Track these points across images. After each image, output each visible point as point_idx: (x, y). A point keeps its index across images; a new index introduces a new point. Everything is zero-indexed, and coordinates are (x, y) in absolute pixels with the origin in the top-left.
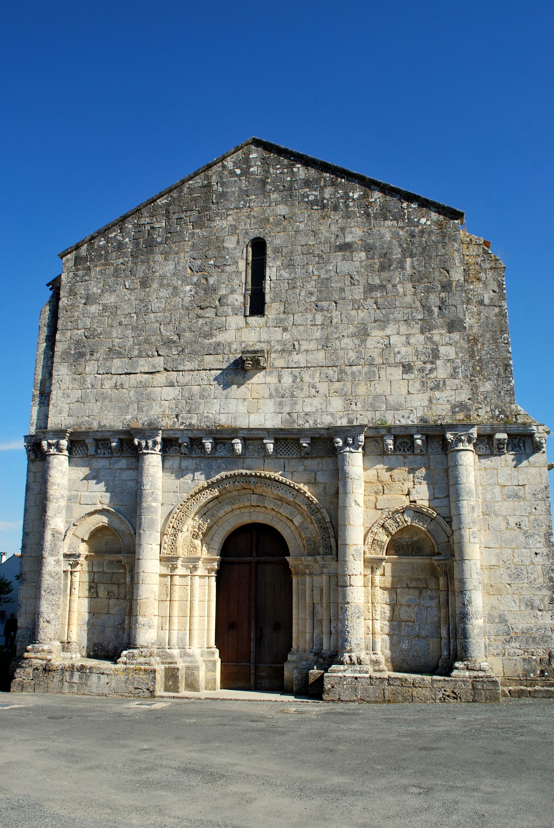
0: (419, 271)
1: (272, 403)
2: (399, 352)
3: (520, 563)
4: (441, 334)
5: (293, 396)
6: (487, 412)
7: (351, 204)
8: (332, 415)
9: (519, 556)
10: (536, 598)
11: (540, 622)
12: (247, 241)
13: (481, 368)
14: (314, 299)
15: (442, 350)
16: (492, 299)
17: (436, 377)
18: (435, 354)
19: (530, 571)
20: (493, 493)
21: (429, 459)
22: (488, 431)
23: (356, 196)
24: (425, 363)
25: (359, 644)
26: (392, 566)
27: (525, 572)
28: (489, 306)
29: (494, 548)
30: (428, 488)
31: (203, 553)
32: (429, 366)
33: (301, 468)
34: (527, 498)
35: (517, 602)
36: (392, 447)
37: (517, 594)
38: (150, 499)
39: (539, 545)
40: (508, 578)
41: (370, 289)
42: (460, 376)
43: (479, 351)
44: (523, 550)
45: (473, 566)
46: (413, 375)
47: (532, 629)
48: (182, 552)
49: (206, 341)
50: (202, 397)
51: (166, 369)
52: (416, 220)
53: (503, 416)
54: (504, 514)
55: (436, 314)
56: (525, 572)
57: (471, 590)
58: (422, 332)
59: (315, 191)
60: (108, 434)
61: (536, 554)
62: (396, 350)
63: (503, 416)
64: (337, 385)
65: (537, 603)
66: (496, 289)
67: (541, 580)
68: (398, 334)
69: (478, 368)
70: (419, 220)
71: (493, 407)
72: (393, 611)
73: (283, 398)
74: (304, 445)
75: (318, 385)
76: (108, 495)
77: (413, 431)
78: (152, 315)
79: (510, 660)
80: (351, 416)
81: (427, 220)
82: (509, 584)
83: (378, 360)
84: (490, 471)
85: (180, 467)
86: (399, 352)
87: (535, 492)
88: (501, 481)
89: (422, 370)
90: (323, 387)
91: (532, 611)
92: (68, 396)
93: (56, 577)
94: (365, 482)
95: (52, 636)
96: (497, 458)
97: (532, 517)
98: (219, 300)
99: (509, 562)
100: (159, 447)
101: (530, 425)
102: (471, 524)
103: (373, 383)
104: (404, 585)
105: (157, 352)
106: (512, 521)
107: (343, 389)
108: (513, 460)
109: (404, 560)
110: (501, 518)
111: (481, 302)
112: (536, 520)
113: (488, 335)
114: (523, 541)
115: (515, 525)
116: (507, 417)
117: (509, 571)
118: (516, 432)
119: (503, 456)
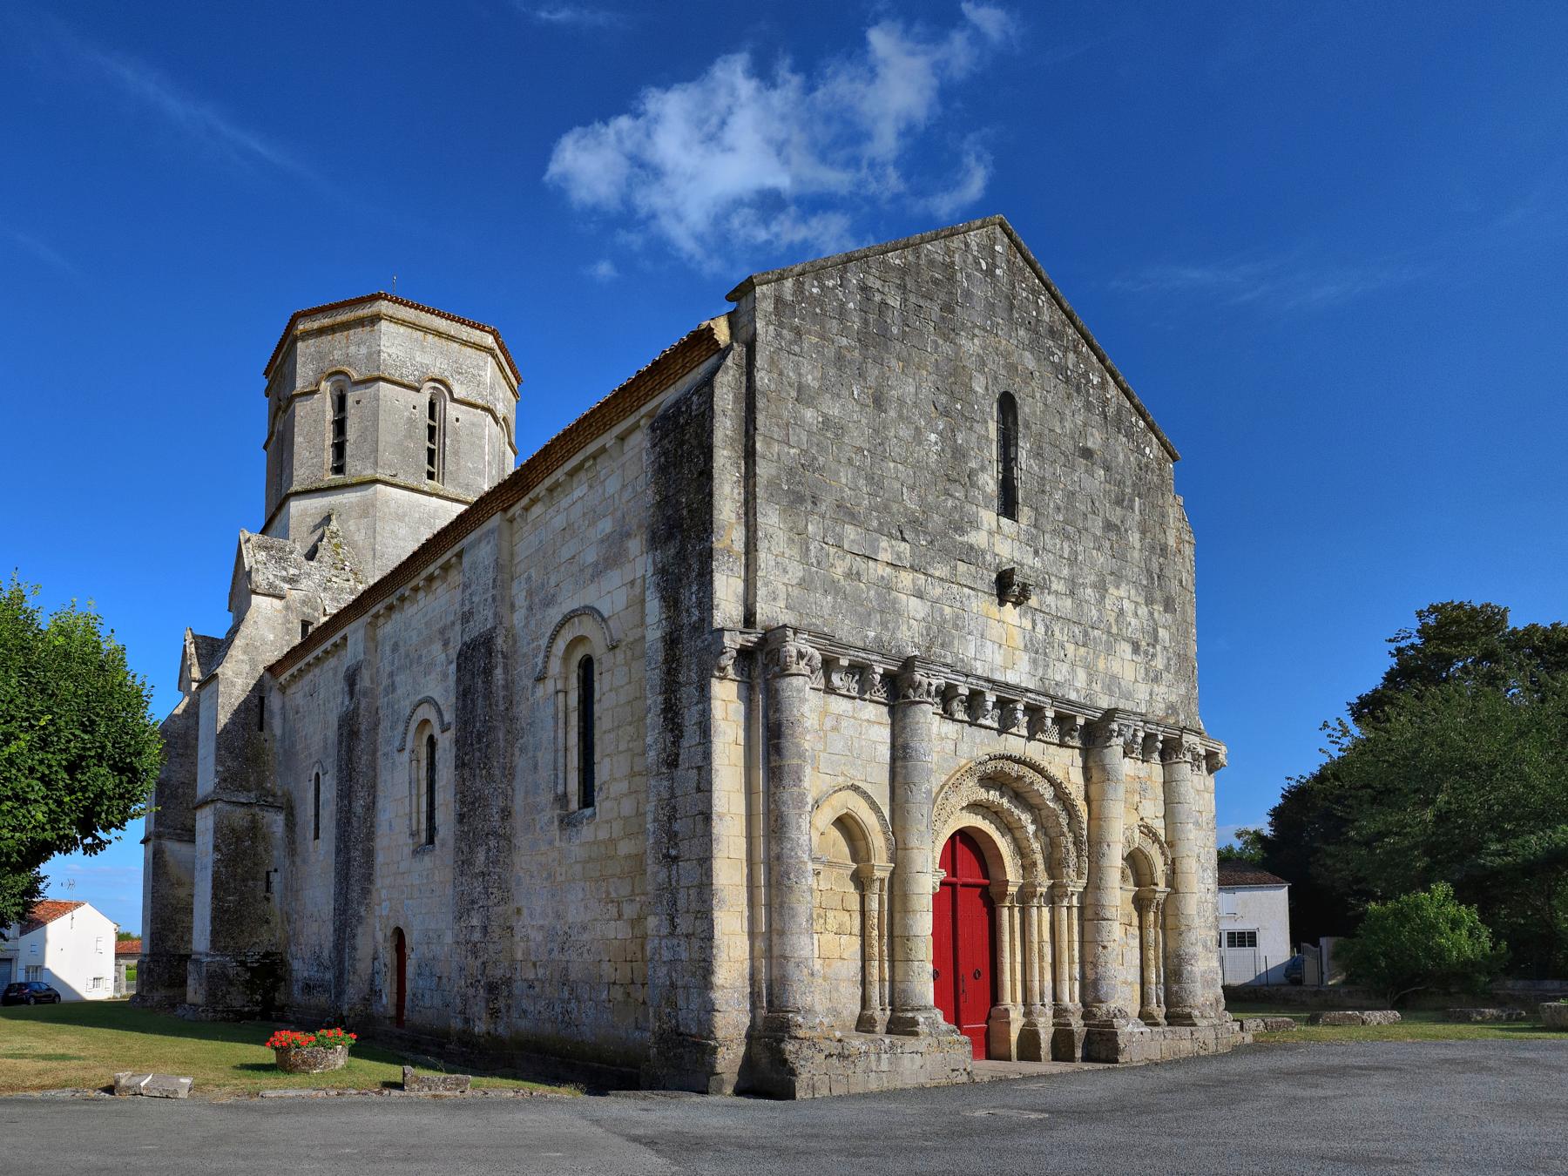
1: (1027, 658)
49: (957, 536)
50: (956, 626)
51: (912, 567)
64: (1082, 650)
78: (892, 465)
92: (785, 571)
98: (969, 477)
105: (901, 532)
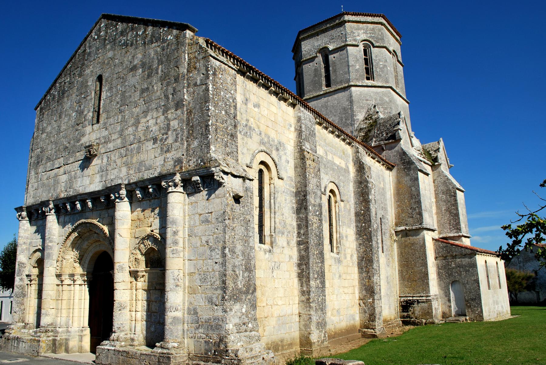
0: (165, 73)
2: (152, 131)
3: (206, 271)
4: (172, 113)
5: (107, 170)
6: (194, 162)
7: (138, 39)
8: (122, 178)
9: (206, 265)
10: (214, 296)
11: (216, 314)
12: (96, 78)
13: (193, 131)
14: (119, 106)
15: (172, 123)
16: (202, 80)
17: (168, 143)
18: (168, 127)
19: (211, 276)
20: (195, 220)
21: (161, 200)
22: (188, 177)
23: (141, 33)
24: (163, 135)
25: (120, 327)
26: (149, 275)
27: (209, 277)
28: (200, 85)
29: (193, 260)
30: (160, 220)
31: (79, 270)
32: (165, 136)
33: (107, 215)
34: (213, 222)
35: (204, 299)
36: (140, 195)
37: (204, 293)
38: (48, 241)
39: (218, 256)
40: (199, 281)
41: (143, 91)
42: (179, 140)
43: (192, 120)
44: (209, 261)
45: (171, 274)
46: (157, 145)
47: (211, 320)
48: (67, 271)
52: (166, 38)
53: (202, 163)
54: (200, 234)
55: (171, 99)
56: (209, 277)
57: (168, 291)
58: (163, 114)
59: (124, 37)
60: (37, 206)
61: (216, 263)
62: (151, 129)
63: (202, 163)
65: (215, 300)
66: (205, 72)
67: (218, 283)
68: (152, 118)
69: (191, 132)
70: (167, 38)
71: (197, 158)
72: (148, 305)
73: (103, 172)
74: (102, 200)
75: (117, 161)
76: (41, 240)
77: (147, 183)
79: (198, 341)
80: (129, 178)
81: (171, 36)
82: (200, 286)
83: (143, 138)
84: (194, 204)
85: (64, 221)
86: (152, 131)
87: (217, 217)
88: (200, 211)
89: (161, 140)
90: (119, 162)
91: (211, 306)
93: (20, 288)
94: (132, 220)
95: (17, 320)
96: (198, 194)
97: (215, 236)
99: (201, 270)
100: (53, 211)
101: (210, 167)
102: (172, 244)
103: (139, 154)
104: (154, 288)
106: (204, 239)
107: (127, 161)
108: (206, 195)
109: (154, 271)
110: (198, 238)
111: (195, 85)
112: (217, 238)
113: (198, 107)
114: (209, 254)
115: (205, 243)
116: (205, 163)
117: (200, 276)
118: (203, 174)
119: (201, 193)
